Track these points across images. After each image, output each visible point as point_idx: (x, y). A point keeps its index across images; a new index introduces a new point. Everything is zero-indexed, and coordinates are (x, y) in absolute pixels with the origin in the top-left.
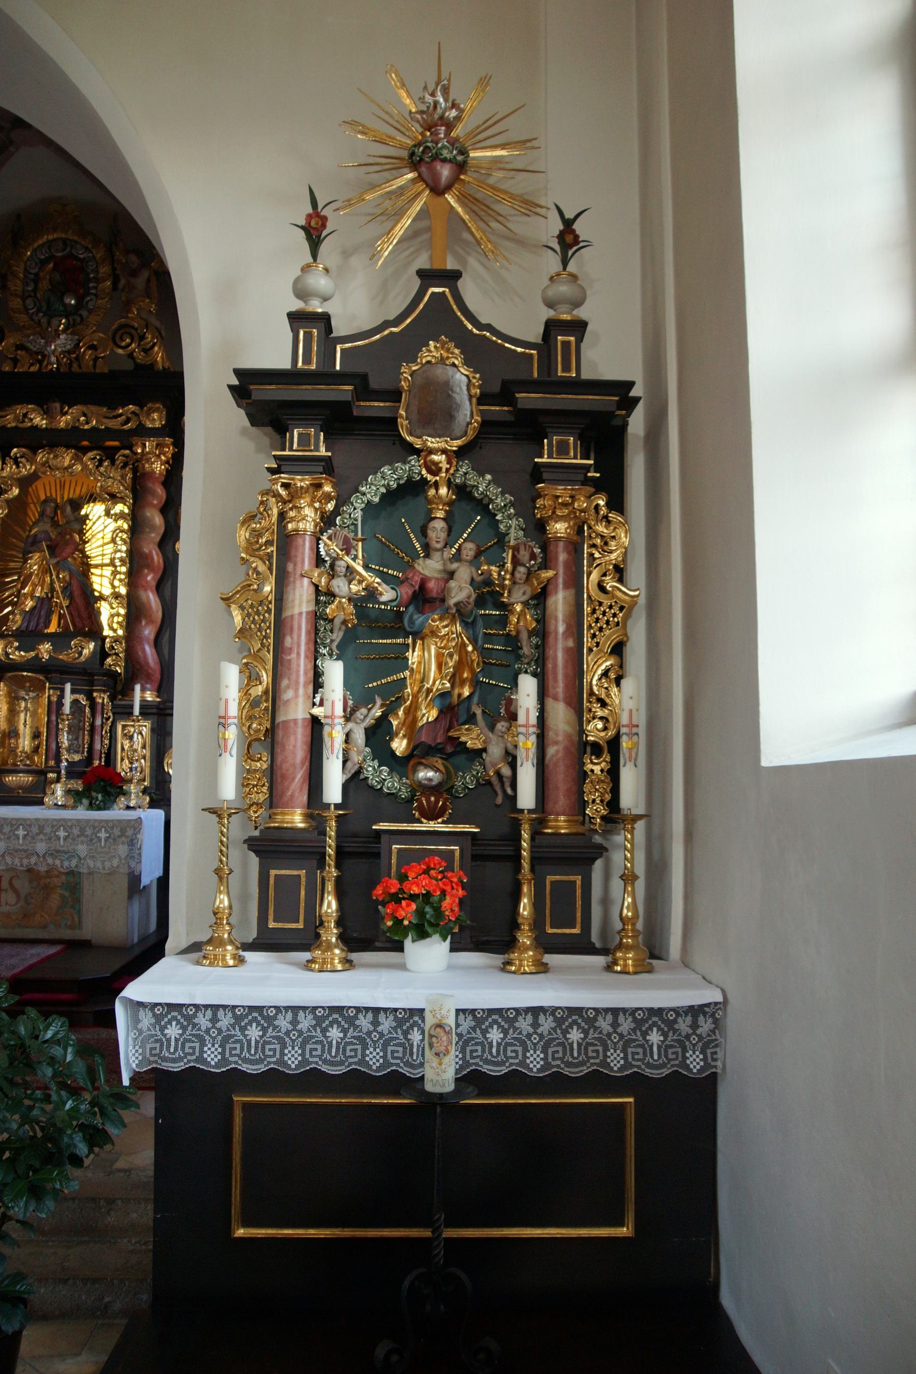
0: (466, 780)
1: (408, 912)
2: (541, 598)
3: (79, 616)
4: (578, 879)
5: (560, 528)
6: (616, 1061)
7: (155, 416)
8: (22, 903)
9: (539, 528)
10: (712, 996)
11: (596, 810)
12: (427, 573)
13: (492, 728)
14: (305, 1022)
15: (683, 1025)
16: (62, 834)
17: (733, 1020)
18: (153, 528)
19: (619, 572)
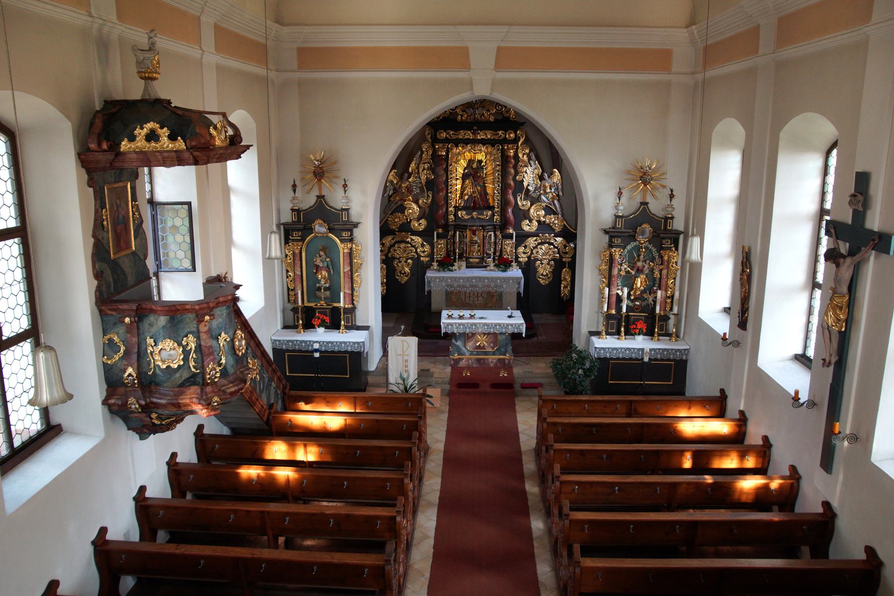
0: (644, 304)
1: (637, 331)
2: (661, 270)
3: (483, 200)
4: (665, 324)
5: (666, 258)
6: (672, 357)
7: (512, 135)
8: (485, 300)
9: (661, 257)
10: (688, 347)
11: (668, 309)
12: (639, 265)
13: (650, 295)
14: (623, 350)
15: (683, 352)
16: (499, 281)
17: (691, 351)
18: (511, 174)
19: (676, 263)
